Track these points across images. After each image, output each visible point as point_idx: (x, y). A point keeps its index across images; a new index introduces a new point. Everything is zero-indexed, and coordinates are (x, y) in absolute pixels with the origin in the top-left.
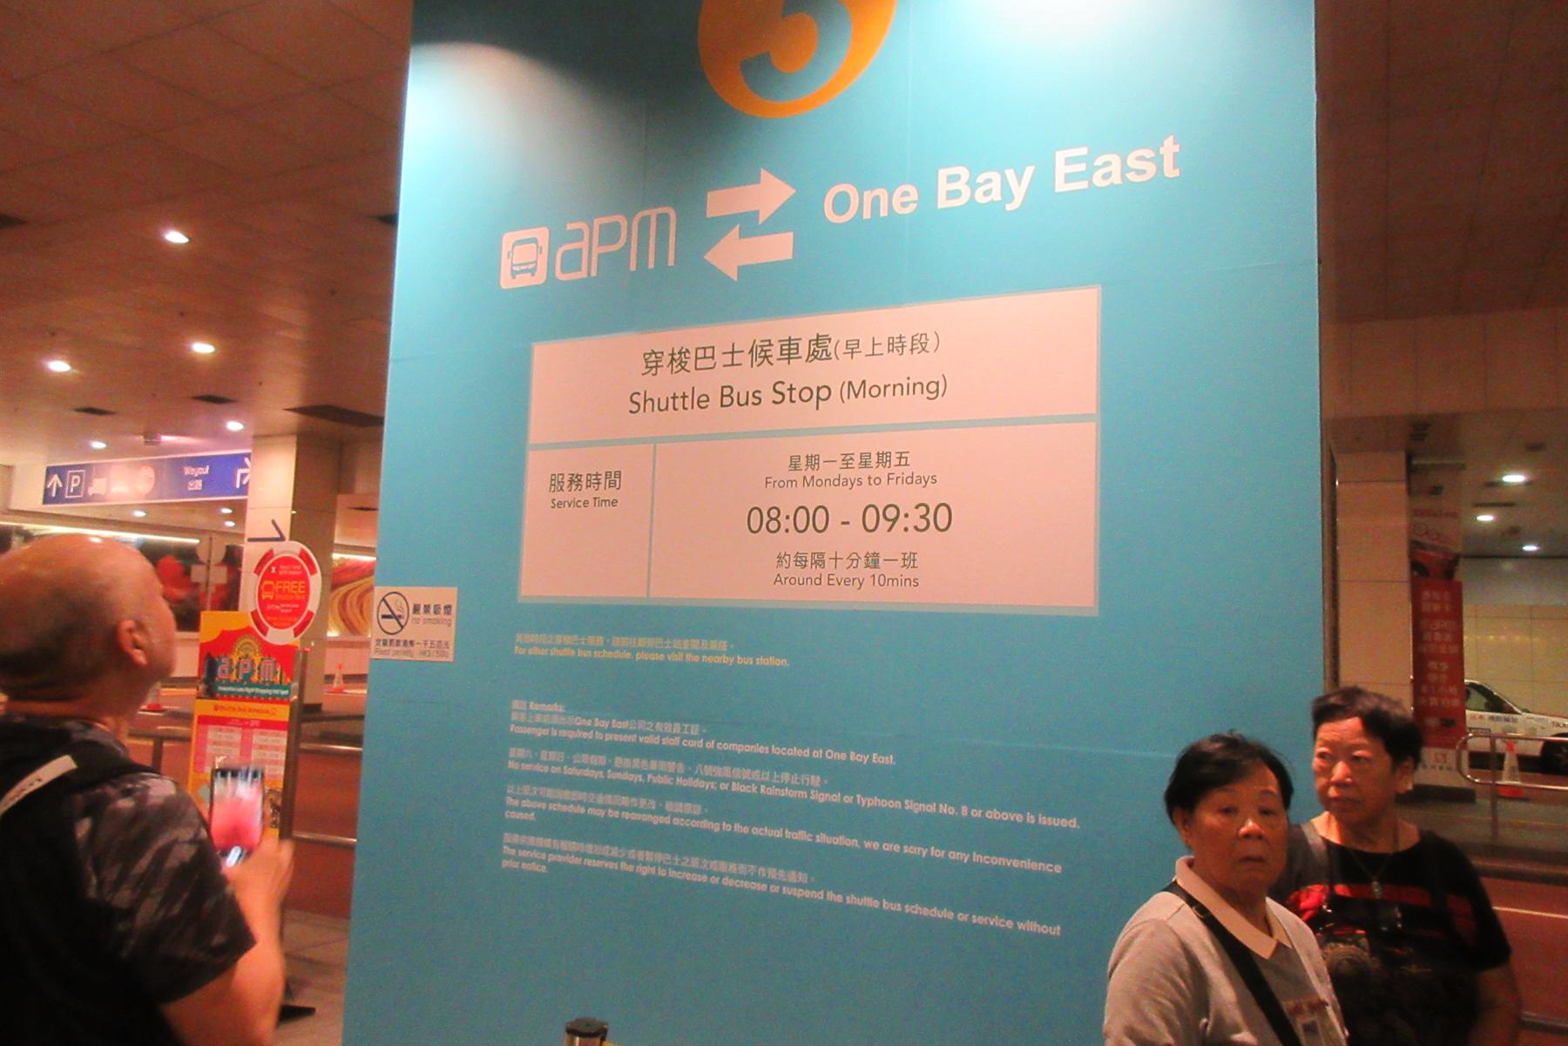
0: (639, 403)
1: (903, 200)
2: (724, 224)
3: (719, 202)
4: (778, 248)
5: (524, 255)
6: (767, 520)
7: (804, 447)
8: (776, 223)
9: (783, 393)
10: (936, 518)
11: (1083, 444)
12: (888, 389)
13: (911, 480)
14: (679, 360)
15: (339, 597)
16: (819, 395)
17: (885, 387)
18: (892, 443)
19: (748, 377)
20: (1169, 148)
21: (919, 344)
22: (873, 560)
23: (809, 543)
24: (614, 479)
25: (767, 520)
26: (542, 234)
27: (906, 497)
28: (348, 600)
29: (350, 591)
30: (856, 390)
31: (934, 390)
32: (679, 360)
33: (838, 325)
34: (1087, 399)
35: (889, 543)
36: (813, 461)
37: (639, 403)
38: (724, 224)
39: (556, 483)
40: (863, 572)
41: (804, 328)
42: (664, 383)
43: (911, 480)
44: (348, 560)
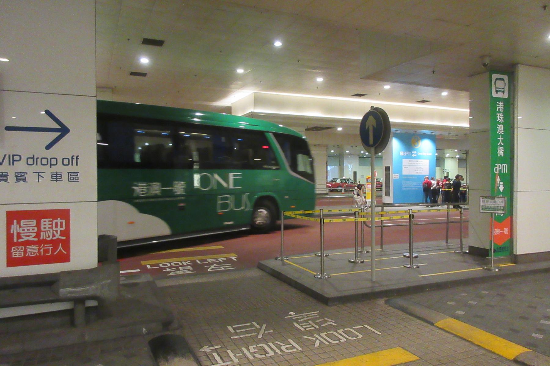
0: (409, 163)
1: (421, 154)
2: (413, 154)
3: (413, 152)
4: (416, 155)
5: (402, 153)
8: (416, 154)
9: (416, 164)
10: (423, 170)
12: (38, 160)
14: (411, 161)
16: (418, 164)
17: (72, 159)
19: (414, 162)
21: (422, 162)
23: (418, 171)
26: (403, 152)
27: (422, 169)
31: (423, 164)
32: (411, 161)
33: (419, 160)
35: (421, 172)
37: (409, 163)
38: (413, 154)
41: (417, 160)
42: (410, 162)
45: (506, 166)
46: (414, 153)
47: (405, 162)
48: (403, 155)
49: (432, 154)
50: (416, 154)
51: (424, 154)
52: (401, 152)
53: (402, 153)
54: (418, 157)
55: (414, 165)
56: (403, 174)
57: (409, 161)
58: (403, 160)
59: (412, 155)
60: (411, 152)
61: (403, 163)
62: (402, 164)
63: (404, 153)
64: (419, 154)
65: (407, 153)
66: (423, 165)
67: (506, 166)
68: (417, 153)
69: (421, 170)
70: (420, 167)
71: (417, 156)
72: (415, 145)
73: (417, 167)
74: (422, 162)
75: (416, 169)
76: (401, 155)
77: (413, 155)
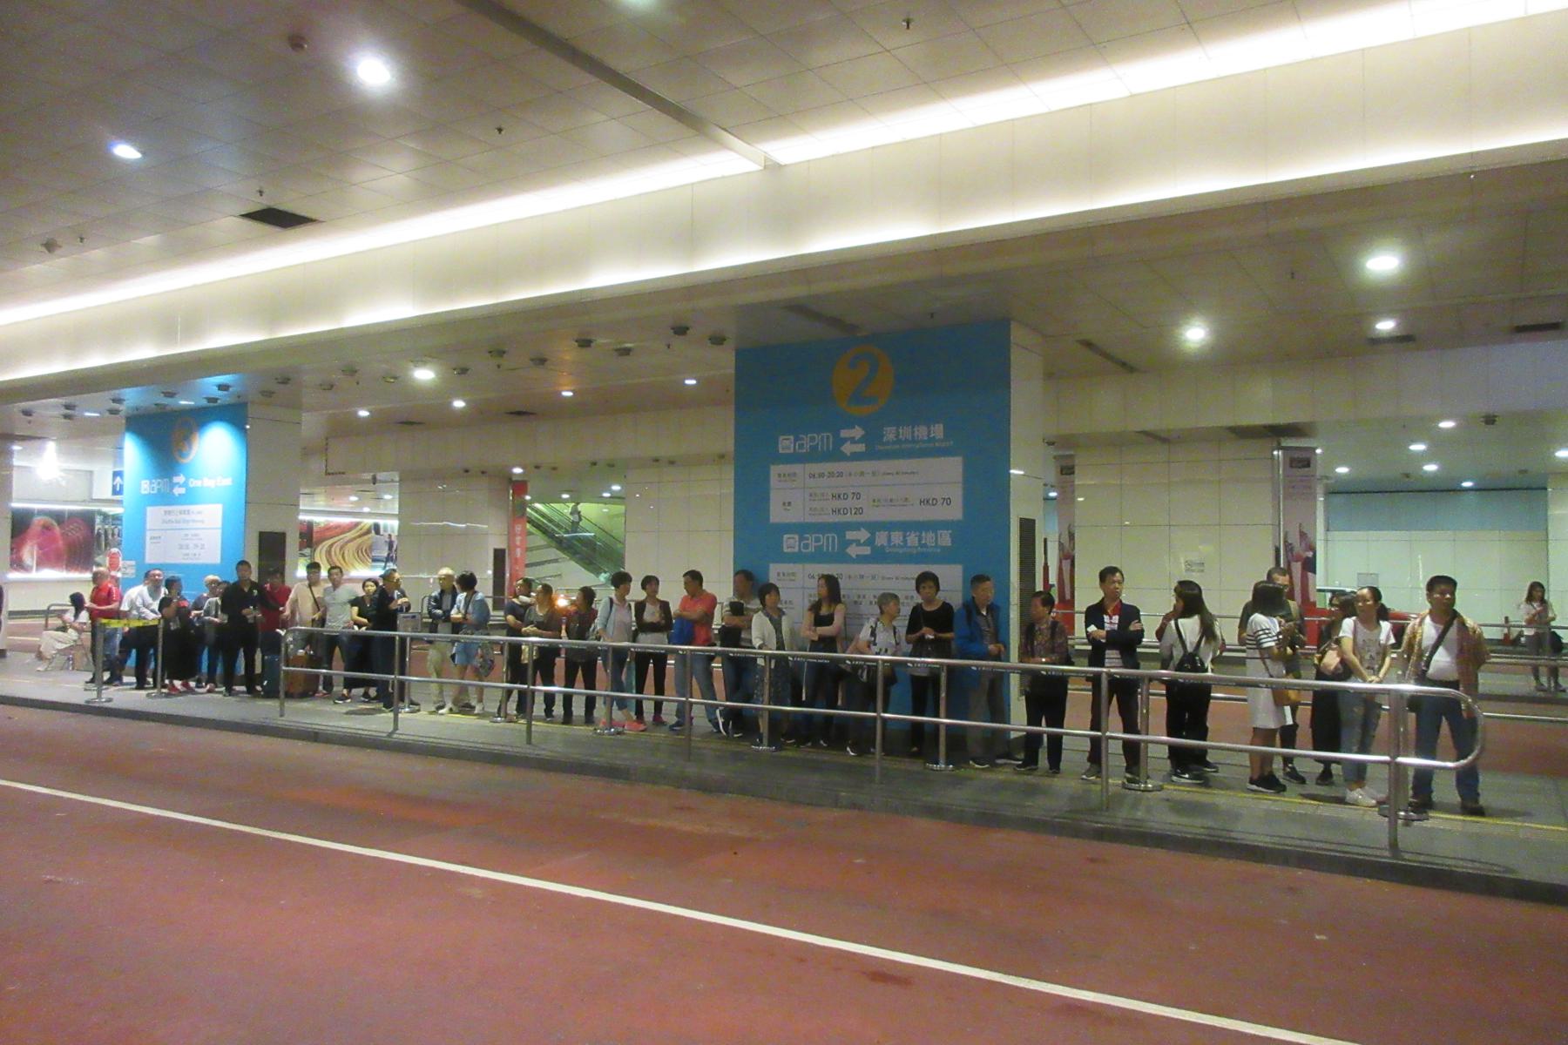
0: (164, 522)
3: (176, 480)
4: (183, 491)
6: (181, 547)
10: (203, 547)
11: (220, 531)
14: (169, 513)
15: (325, 549)
16: (188, 522)
21: (199, 513)
22: (195, 555)
23: (187, 551)
25: (181, 547)
26: (148, 482)
28: (333, 549)
29: (335, 542)
30: (194, 521)
31: (202, 522)
33: (193, 508)
34: (220, 525)
37: (164, 522)
39: (151, 538)
44: (332, 522)
45: (833, 538)
46: (178, 483)
47: (154, 514)
48: (146, 492)
49: (233, 481)
50: (185, 485)
51: (208, 483)
52: (143, 482)
53: (146, 487)
54: (190, 498)
55: (178, 526)
57: (165, 512)
59: (172, 489)
60: (171, 481)
61: (148, 519)
62: (144, 522)
63: (151, 483)
64: (193, 483)
65: (159, 483)
66: (203, 526)
67: (833, 538)
69: (196, 546)
70: (196, 535)
71: (187, 490)
72: (180, 451)
73: (187, 535)
74: (199, 513)
76: (143, 492)
77: (177, 491)
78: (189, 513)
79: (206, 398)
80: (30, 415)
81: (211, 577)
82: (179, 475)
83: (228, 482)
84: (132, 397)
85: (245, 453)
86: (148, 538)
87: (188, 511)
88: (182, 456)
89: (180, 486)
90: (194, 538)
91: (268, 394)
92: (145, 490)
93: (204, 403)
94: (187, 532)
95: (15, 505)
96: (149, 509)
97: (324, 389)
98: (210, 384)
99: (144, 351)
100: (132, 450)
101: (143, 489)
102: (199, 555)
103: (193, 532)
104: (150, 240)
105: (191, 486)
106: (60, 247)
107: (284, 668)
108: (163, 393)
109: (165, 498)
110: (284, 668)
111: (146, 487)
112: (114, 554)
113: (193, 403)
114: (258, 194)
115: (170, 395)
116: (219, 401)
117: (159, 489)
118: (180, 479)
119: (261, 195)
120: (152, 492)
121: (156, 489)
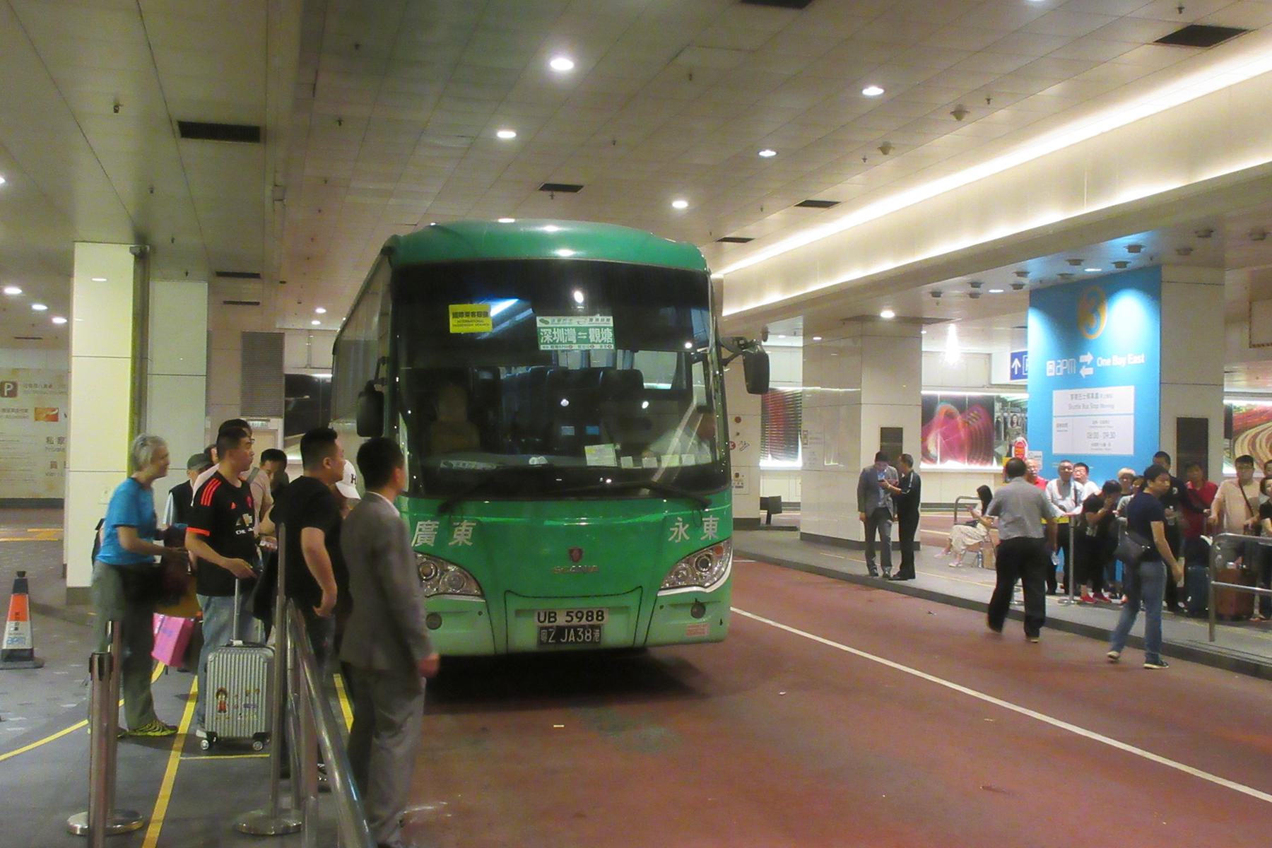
0: (1071, 407)
3: (1083, 359)
4: (1090, 371)
6: (1090, 436)
7: (1095, 418)
11: (1132, 418)
13: (1110, 427)
14: (1076, 397)
15: (1248, 437)
16: (1096, 407)
18: (1106, 418)
20: (1143, 356)
21: (1108, 396)
23: (1096, 441)
24: (1066, 425)
25: (1090, 436)
26: (1053, 362)
28: (1258, 441)
29: (1259, 433)
30: (1103, 406)
31: (1112, 406)
36: (1096, 422)
38: (1083, 364)
40: (1103, 448)
42: (1075, 402)
43: (1110, 427)
44: (1255, 406)
46: (1086, 363)
47: (1061, 398)
48: (1053, 374)
50: (1093, 364)
53: (1052, 368)
56: (1054, 452)
58: (1055, 393)
59: (1078, 370)
60: (1078, 359)
64: (1103, 362)
68: (1095, 359)
69: (1106, 435)
71: (1094, 370)
75: (1093, 431)
77: (1085, 372)
78: (1097, 397)
79: (1115, 263)
80: (939, 296)
81: (1124, 470)
82: (1086, 354)
83: (1140, 359)
84: (1037, 269)
85: (1159, 325)
86: (1054, 428)
87: (1097, 394)
88: (1089, 330)
89: (1088, 367)
90: (1103, 425)
91: (1186, 251)
92: (1051, 371)
93: (1112, 268)
94: (1095, 418)
95: (924, 392)
96: (1055, 393)
97: (1255, 240)
98: (1119, 247)
99: (1050, 216)
100: (1037, 327)
101: (1048, 371)
102: (1109, 445)
103: (1102, 418)
104: (1053, 91)
105: (1099, 365)
106: (967, 112)
107: (1213, 582)
108: (1069, 261)
109: (1071, 380)
110: (1213, 582)
111: (1052, 368)
112: (1020, 443)
113: (1100, 270)
114: (1178, 11)
115: (1076, 262)
116: (1128, 265)
117: (1065, 370)
118: (1087, 358)
119: (1180, 12)
120: (1058, 374)
121: (1061, 370)
